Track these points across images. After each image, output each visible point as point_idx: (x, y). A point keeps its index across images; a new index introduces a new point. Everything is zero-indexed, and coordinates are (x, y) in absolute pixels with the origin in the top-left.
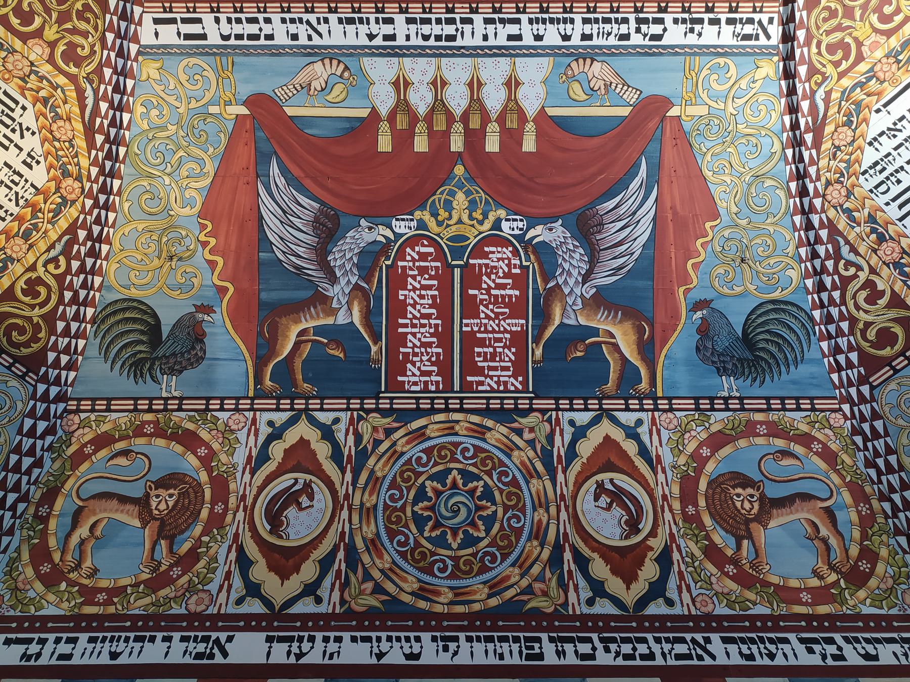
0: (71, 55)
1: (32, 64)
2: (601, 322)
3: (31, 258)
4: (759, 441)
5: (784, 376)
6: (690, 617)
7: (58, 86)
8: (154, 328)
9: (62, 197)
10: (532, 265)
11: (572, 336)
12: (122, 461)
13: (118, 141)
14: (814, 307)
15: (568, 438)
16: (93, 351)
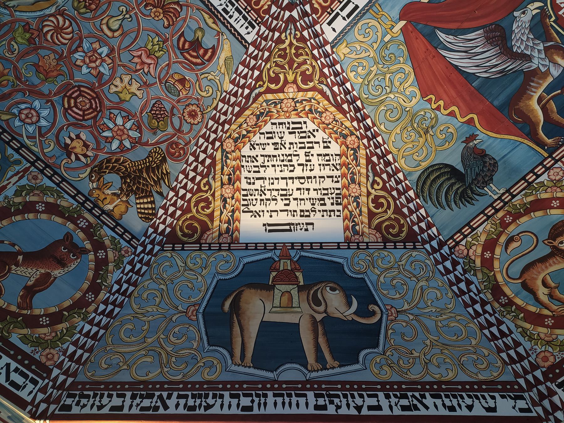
0: (307, 78)
1: (293, 99)
3: (364, 190)
7: (311, 98)
8: (453, 171)
9: (352, 149)
12: (514, 245)
13: (354, 100)
16: (432, 210)
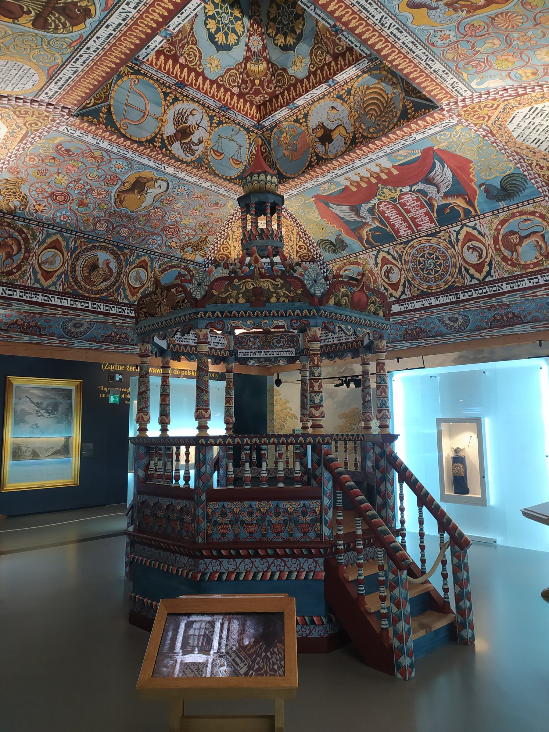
2: (450, 200)
4: (517, 218)
5: (521, 195)
6: (498, 279)
8: (331, 243)
10: (420, 196)
11: (442, 209)
12: (346, 272)
13: (291, 215)
14: (524, 171)
15: (455, 235)
16: (322, 251)
